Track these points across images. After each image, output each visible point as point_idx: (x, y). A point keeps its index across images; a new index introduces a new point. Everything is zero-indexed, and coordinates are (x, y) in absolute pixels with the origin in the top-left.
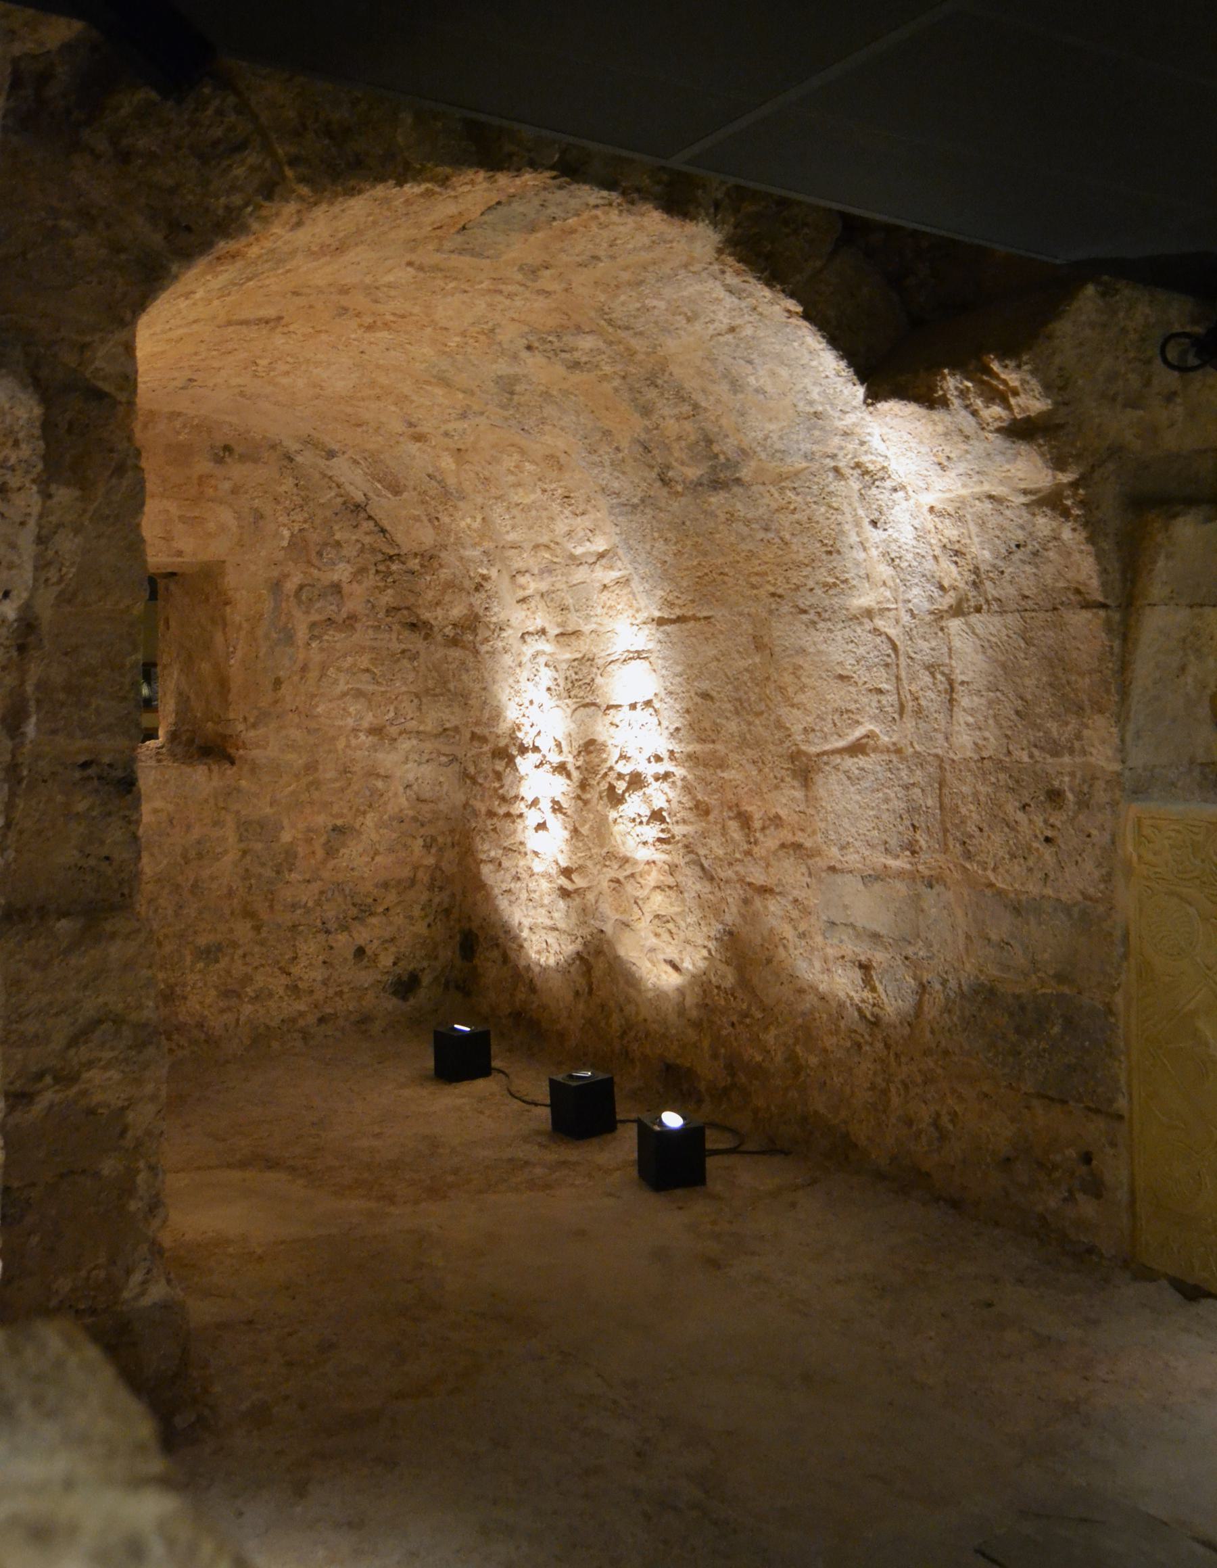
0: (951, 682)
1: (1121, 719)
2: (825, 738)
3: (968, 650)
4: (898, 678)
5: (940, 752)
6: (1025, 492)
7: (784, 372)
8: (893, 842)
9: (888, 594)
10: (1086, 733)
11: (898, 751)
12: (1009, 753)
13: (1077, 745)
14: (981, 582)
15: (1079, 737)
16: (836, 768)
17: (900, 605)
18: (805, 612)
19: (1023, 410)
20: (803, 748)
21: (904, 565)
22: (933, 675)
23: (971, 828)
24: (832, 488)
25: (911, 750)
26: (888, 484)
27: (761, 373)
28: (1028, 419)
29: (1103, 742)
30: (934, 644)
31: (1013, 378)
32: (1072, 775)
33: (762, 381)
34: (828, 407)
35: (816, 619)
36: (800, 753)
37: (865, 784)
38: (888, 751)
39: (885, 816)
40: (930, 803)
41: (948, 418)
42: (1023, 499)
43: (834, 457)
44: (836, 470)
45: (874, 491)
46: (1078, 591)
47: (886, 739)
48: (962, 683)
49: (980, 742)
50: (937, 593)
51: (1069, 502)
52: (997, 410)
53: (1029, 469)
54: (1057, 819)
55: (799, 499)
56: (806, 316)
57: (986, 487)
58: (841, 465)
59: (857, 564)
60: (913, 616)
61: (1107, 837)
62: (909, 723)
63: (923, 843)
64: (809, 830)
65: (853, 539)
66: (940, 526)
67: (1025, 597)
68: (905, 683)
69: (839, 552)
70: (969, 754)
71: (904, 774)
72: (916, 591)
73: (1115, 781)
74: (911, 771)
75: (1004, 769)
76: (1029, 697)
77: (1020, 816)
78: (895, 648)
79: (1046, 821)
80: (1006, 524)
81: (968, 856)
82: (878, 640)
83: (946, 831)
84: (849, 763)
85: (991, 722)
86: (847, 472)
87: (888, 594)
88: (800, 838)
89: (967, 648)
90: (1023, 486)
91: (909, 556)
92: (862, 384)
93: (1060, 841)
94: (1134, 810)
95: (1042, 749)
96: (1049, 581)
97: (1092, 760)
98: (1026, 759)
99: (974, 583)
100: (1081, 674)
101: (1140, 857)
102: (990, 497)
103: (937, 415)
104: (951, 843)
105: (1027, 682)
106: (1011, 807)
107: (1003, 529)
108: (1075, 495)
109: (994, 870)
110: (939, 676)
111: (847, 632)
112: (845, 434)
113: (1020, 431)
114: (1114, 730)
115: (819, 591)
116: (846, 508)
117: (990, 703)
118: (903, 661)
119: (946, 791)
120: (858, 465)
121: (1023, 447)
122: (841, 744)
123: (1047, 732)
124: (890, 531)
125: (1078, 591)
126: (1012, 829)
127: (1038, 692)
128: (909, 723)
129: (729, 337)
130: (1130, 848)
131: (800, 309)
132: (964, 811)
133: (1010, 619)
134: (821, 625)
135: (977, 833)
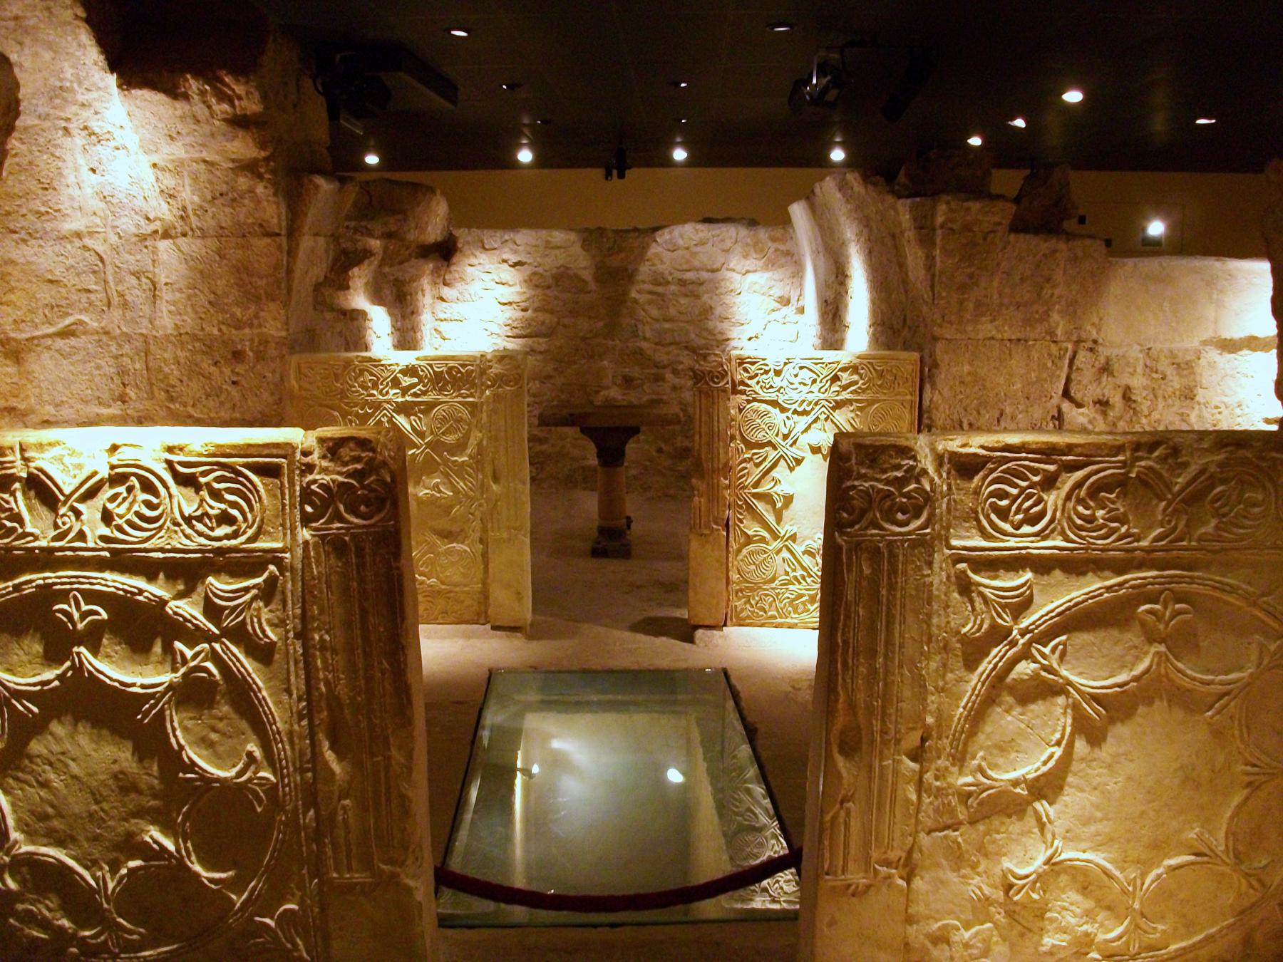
0: (154, 284)
1: (286, 305)
2: (36, 327)
3: (174, 261)
4: (105, 281)
5: (144, 331)
6: (233, 161)
7: (47, 55)
8: (106, 396)
9: (98, 221)
10: (262, 314)
11: (107, 333)
12: (202, 329)
13: (256, 322)
14: (188, 216)
15: (256, 316)
16: (48, 348)
17: (109, 230)
18: (15, 232)
19: (242, 109)
20: (12, 335)
21: (115, 201)
22: (138, 278)
23: (173, 381)
24: (59, 142)
25: (118, 331)
26: (112, 144)
27: (27, 51)
28: (245, 116)
29: (275, 319)
30: (139, 257)
31: (239, 89)
32: (252, 340)
33: (23, 59)
34: (75, 85)
35: (27, 237)
36: (9, 339)
37: (76, 358)
38: (98, 333)
39: (97, 379)
40: (137, 366)
41: (187, 107)
42: (231, 165)
43: (67, 120)
44: (66, 129)
45: (99, 147)
46: (261, 225)
47: (96, 324)
48: (166, 284)
49: (179, 323)
50: (143, 222)
51: (262, 170)
52: (225, 107)
53: (243, 147)
54: (240, 369)
55: (23, 147)
56: (87, 21)
57: (205, 155)
58: (70, 126)
59: (72, 198)
60: (120, 238)
61: (278, 376)
62: (116, 314)
63: (132, 395)
64: (22, 396)
65: (71, 179)
66: (161, 177)
67: (222, 228)
68: (112, 284)
69: (55, 189)
70: (169, 331)
71: (113, 349)
72: (124, 220)
73: (280, 343)
74: (120, 346)
75: (198, 340)
76: (219, 292)
77: (213, 369)
78: (102, 260)
79: (233, 371)
80: (215, 180)
81: (172, 399)
82: (87, 254)
83: (151, 384)
84: (60, 343)
85: (189, 310)
86: (75, 131)
87: (98, 221)
88: (13, 402)
89: (169, 260)
90: (233, 157)
91: (121, 196)
92: (112, 73)
93: (244, 382)
94: (294, 360)
95: (229, 325)
96: (242, 218)
97: (265, 330)
98: (216, 332)
99: (182, 217)
100: (261, 278)
101: (300, 387)
102: (205, 161)
103: (178, 104)
104: (156, 392)
105: (219, 282)
106: (206, 365)
107: (210, 182)
108: (267, 165)
109: (193, 406)
110: (144, 280)
111: (57, 248)
112: (83, 105)
113: (239, 122)
114: (282, 312)
115: (31, 217)
116: (68, 157)
117: (189, 298)
118: (110, 270)
119: (151, 357)
120: (86, 128)
121: (241, 133)
122: (52, 330)
123: (233, 315)
124: (107, 177)
125: (261, 225)
126: (209, 378)
127: (227, 289)
128: (116, 314)
129: (12, 24)
130: (293, 382)
131: (84, 15)
132: (166, 369)
133: (209, 242)
134: (32, 242)
135: (178, 383)
